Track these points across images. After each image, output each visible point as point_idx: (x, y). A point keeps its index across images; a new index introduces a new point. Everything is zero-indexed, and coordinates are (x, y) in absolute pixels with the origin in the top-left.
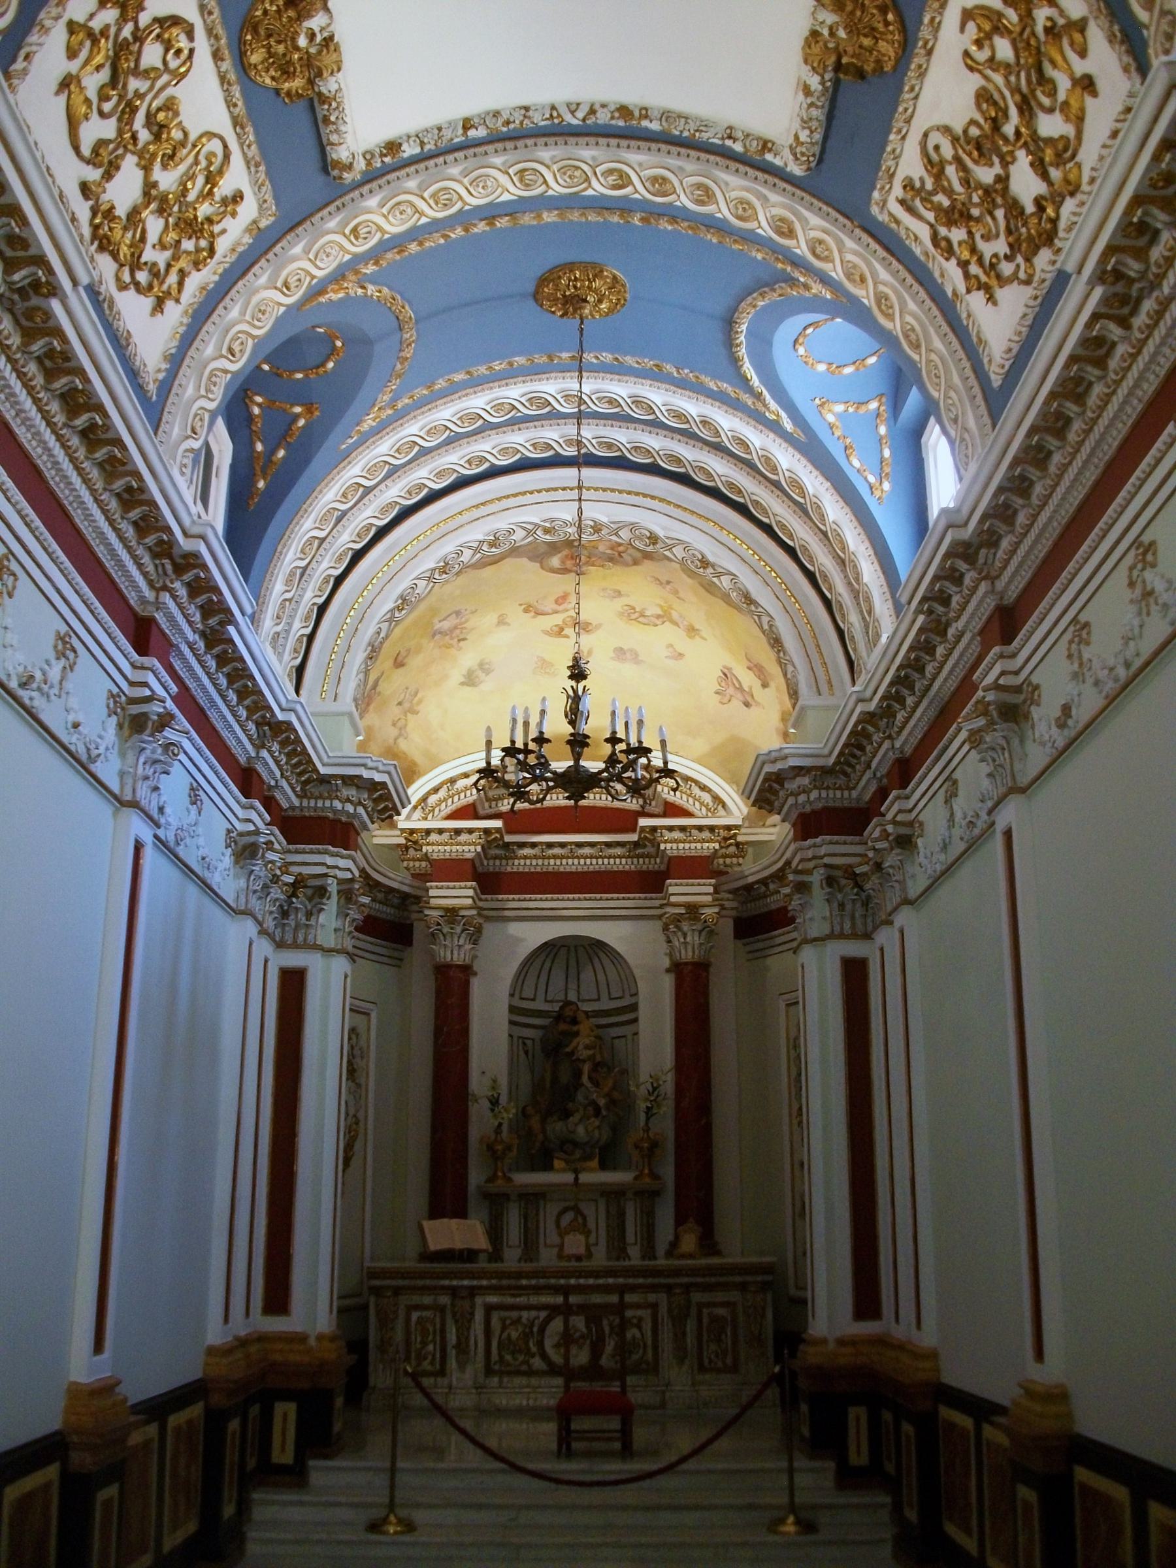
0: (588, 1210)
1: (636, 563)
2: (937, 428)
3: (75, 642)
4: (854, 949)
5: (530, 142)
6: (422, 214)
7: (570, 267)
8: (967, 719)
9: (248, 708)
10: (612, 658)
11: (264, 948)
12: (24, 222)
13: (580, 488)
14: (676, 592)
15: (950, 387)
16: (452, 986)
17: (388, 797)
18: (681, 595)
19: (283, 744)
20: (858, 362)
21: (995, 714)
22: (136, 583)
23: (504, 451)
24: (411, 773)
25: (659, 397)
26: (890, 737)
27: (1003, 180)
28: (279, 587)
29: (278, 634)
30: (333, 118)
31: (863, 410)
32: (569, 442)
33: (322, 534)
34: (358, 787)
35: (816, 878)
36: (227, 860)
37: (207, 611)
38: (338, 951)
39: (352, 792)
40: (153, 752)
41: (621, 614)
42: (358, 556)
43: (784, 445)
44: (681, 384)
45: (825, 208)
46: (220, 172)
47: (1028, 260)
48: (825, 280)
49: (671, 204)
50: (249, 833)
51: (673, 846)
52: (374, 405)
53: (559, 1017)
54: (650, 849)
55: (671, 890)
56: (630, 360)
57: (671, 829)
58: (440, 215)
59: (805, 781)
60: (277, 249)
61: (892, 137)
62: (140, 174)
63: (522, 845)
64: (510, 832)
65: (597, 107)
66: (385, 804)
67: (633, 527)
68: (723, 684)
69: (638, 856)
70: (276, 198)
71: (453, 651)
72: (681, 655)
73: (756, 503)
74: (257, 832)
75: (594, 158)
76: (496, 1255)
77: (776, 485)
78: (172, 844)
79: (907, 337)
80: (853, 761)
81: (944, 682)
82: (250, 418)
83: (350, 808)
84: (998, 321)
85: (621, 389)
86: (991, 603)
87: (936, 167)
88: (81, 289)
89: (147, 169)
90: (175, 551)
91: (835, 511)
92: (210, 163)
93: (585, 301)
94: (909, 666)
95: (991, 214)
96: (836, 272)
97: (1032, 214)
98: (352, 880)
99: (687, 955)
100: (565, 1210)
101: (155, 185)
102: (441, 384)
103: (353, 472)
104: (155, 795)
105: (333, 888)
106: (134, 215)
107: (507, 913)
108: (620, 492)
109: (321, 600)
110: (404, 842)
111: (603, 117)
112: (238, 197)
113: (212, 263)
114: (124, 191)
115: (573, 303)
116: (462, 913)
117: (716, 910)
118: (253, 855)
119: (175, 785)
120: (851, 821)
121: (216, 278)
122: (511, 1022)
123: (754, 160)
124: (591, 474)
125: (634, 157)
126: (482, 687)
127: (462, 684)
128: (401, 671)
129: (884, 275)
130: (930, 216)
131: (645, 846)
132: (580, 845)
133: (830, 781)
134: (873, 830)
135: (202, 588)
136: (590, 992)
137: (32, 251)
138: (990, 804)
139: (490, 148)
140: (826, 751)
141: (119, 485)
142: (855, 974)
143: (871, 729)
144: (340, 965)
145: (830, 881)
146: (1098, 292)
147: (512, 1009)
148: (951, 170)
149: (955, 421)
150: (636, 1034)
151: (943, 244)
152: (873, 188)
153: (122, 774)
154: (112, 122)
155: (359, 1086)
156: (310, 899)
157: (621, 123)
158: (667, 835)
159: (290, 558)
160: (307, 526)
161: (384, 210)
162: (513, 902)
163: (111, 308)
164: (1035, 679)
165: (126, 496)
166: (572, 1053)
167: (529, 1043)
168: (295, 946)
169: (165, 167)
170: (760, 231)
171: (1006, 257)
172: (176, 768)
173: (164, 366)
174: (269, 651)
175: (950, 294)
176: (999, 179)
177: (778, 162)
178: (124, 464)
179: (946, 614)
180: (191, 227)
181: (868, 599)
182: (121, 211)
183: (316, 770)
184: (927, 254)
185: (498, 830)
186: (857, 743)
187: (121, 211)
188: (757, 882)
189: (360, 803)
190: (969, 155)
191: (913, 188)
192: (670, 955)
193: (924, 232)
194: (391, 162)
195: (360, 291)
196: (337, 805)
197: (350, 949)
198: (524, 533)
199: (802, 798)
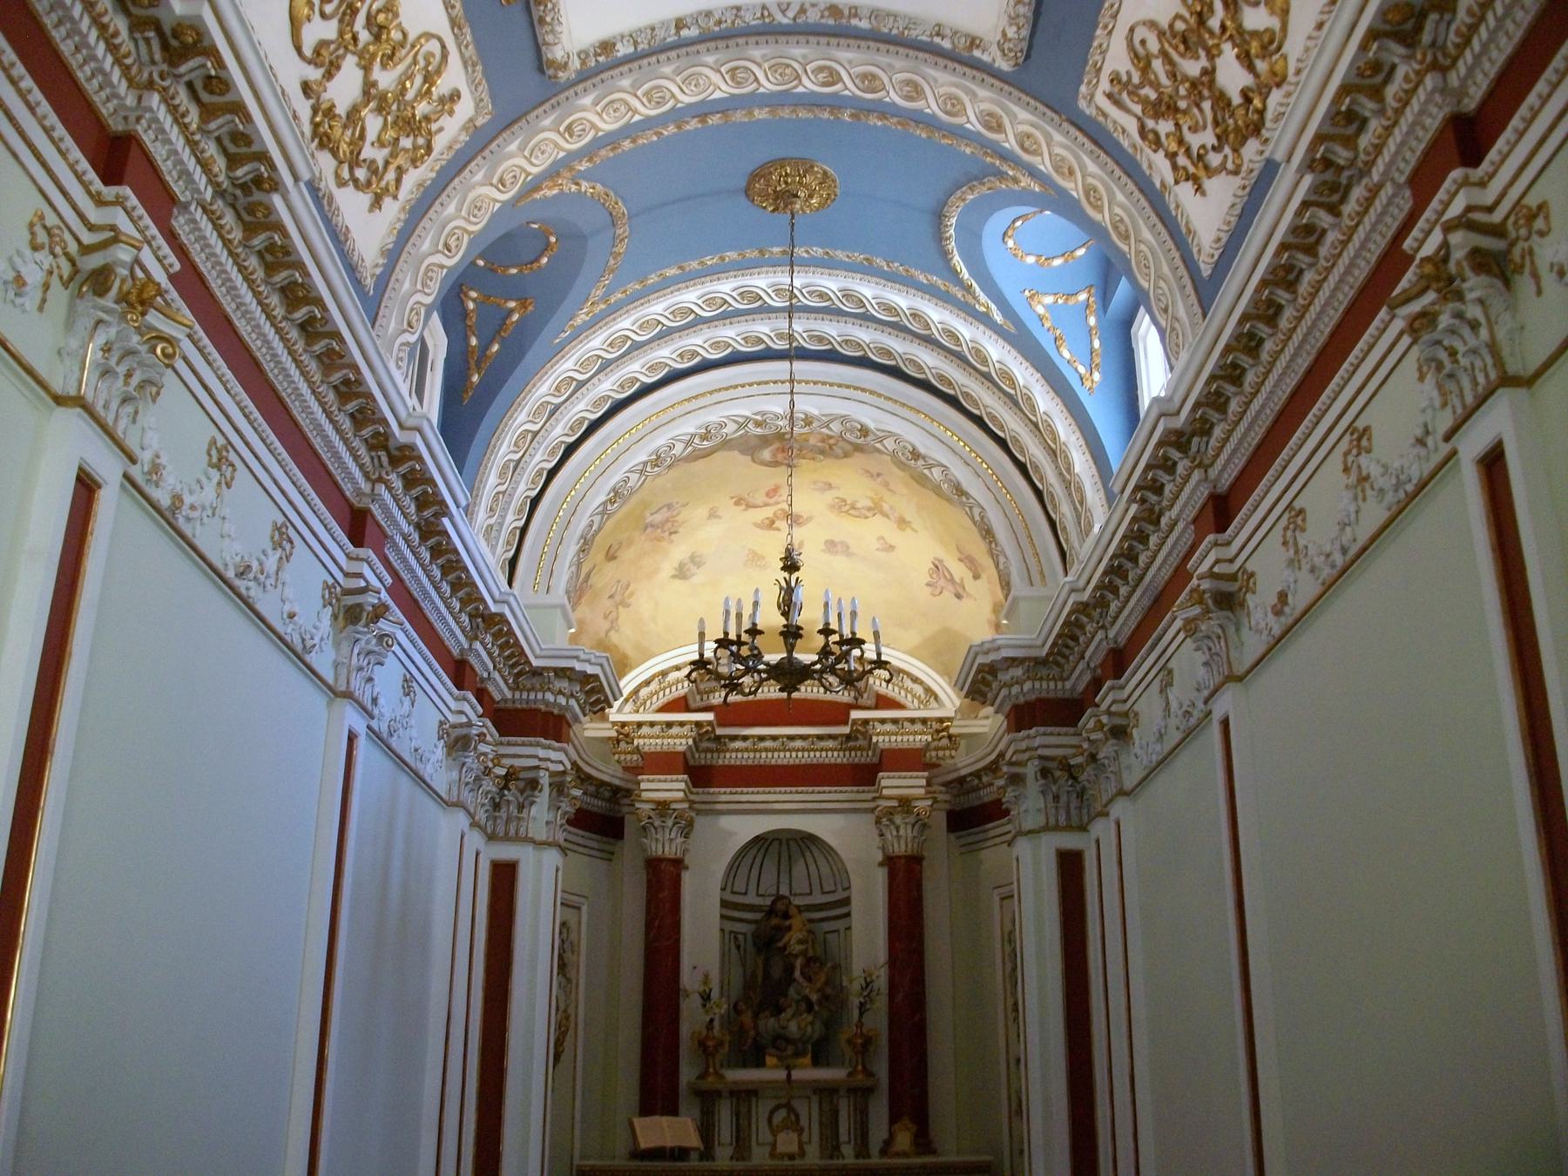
0: (801, 1107)
1: (846, 455)
2: (1147, 317)
3: (291, 532)
4: (1070, 841)
5: (741, 41)
6: (636, 112)
7: (781, 162)
8: (1181, 608)
9: (461, 600)
11: (475, 840)
12: (248, 118)
13: (792, 381)
14: (886, 485)
15: (1159, 277)
16: (663, 881)
17: (601, 689)
18: (892, 486)
19: (496, 636)
20: (1067, 254)
21: (1210, 602)
22: (352, 474)
23: (716, 345)
24: (623, 666)
25: (868, 290)
26: (1103, 627)
27: (1209, 73)
28: (492, 479)
29: (491, 526)
30: (548, 19)
31: (1072, 302)
32: (780, 336)
33: (535, 428)
34: (570, 680)
35: (1031, 770)
36: (440, 752)
37: (422, 503)
38: (550, 844)
39: (563, 684)
40: (368, 642)
41: (832, 507)
42: (570, 449)
43: (994, 337)
44: (891, 278)
45: (1032, 102)
46: (438, 72)
47: (1235, 150)
48: (1033, 173)
49: (880, 100)
50: (461, 725)
51: (884, 739)
52: (587, 300)
53: (771, 911)
54: (861, 742)
55: (884, 783)
56: (840, 255)
57: (883, 721)
58: (653, 113)
59: (1018, 672)
60: (493, 146)
61: (1099, 32)
62: (360, 74)
63: (734, 738)
64: (722, 724)
65: (807, 6)
66: (596, 695)
67: (844, 419)
69: (850, 750)
70: (493, 97)
71: (664, 544)
72: (892, 548)
73: (967, 395)
74: (469, 724)
75: (804, 57)
76: (707, 1154)
77: (987, 377)
78: (385, 735)
79: (1116, 228)
80: (1067, 652)
81: (1158, 571)
82: (465, 314)
83: (562, 701)
84: (1206, 211)
85: (832, 284)
86: (1204, 492)
87: (1142, 62)
88: (302, 185)
89: (367, 69)
90: (391, 444)
91: (1045, 402)
92: (428, 63)
93: (796, 196)
94: (1122, 555)
95: (1198, 106)
96: (1044, 165)
97: (1240, 106)
98: (564, 773)
99: (900, 849)
100: (777, 1108)
101: (374, 84)
102: (653, 279)
103: (567, 366)
104: (369, 686)
105: (545, 780)
106: (354, 114)
107: (718, 807)
108: (831, 385)
109: (534, 493)
110: (614, 734)
111: (813, 16)
112: (455, 96)
113: (429, 161)
114: (344, 89)
115: (783, 199)
116: (674, 806)
117: (929, 802)
118: (466, 747)
119: (388, 677)
120: (1066, 712)
121: (433, 175)
122: (722, 917)
123: (961, 56)
124: (802, 368)
125: (845, 55)
126: (695, 580)
127: (674, 577)
128: (613, 564)
129: (1092, 167)
130: (1138, 109)
131: (857, 739)
132: (791, 738)
133: (1044, 672)
134: (1088, 721)
135: (416, 480)
136: (802, 885)
137: (255, 148)
138: (1206, 693)
139: (702, 47)
140: (1039, 642)
141: (336, 377)
142: (1070, 866)
143: (1085, 619)
144: (552, 858)
145: (1045, 773)
146: (1308, 180)
147: (725, 904)
148: (1157, 65)
149: (1166, 310)
150: (849, 928)
151: (1151, 136)
152: (1081, 82)
153: (336, 665)
154: (334, 24)
155: (569, 980)
156: (522, 792)
157: (831, 22)
158: (879, 728)
159: (504, 451)
160: (521, 419)
161: (598, 109)
162: (724, 795)
163: (330, 204)
164: (1250, 567)
165: (343, 389)
166: (785, 948)
167: (741, 937)
168: (507, 838)
169: (384, 66)
170: (968, 126)
171: (1213, 148)
172: (390, 660)
173: (381, 261)
174: (483, 544)
175: (1158, 185)
176: (1205, 72)
177: (986, 58)
178: (342, 357)
179: (1159, 503)
180: (409, 125)
181: (1080, 490)
182: (341, 110)
183: (528, 662)
184: (1134, 146)
185: (710, 723)
186: (1071, 633)
187: (341, 110)
188: (971, 774)
189: (572, 695)
190: (1176, 48)
191: (1119, 82)
192: (883, 848)
193: (1131, 125)
194: (605, 61)
195: (574, 188)
196: (550, 697)
197: (562, 842)
198: (735, 426)
199: (1015, 689)
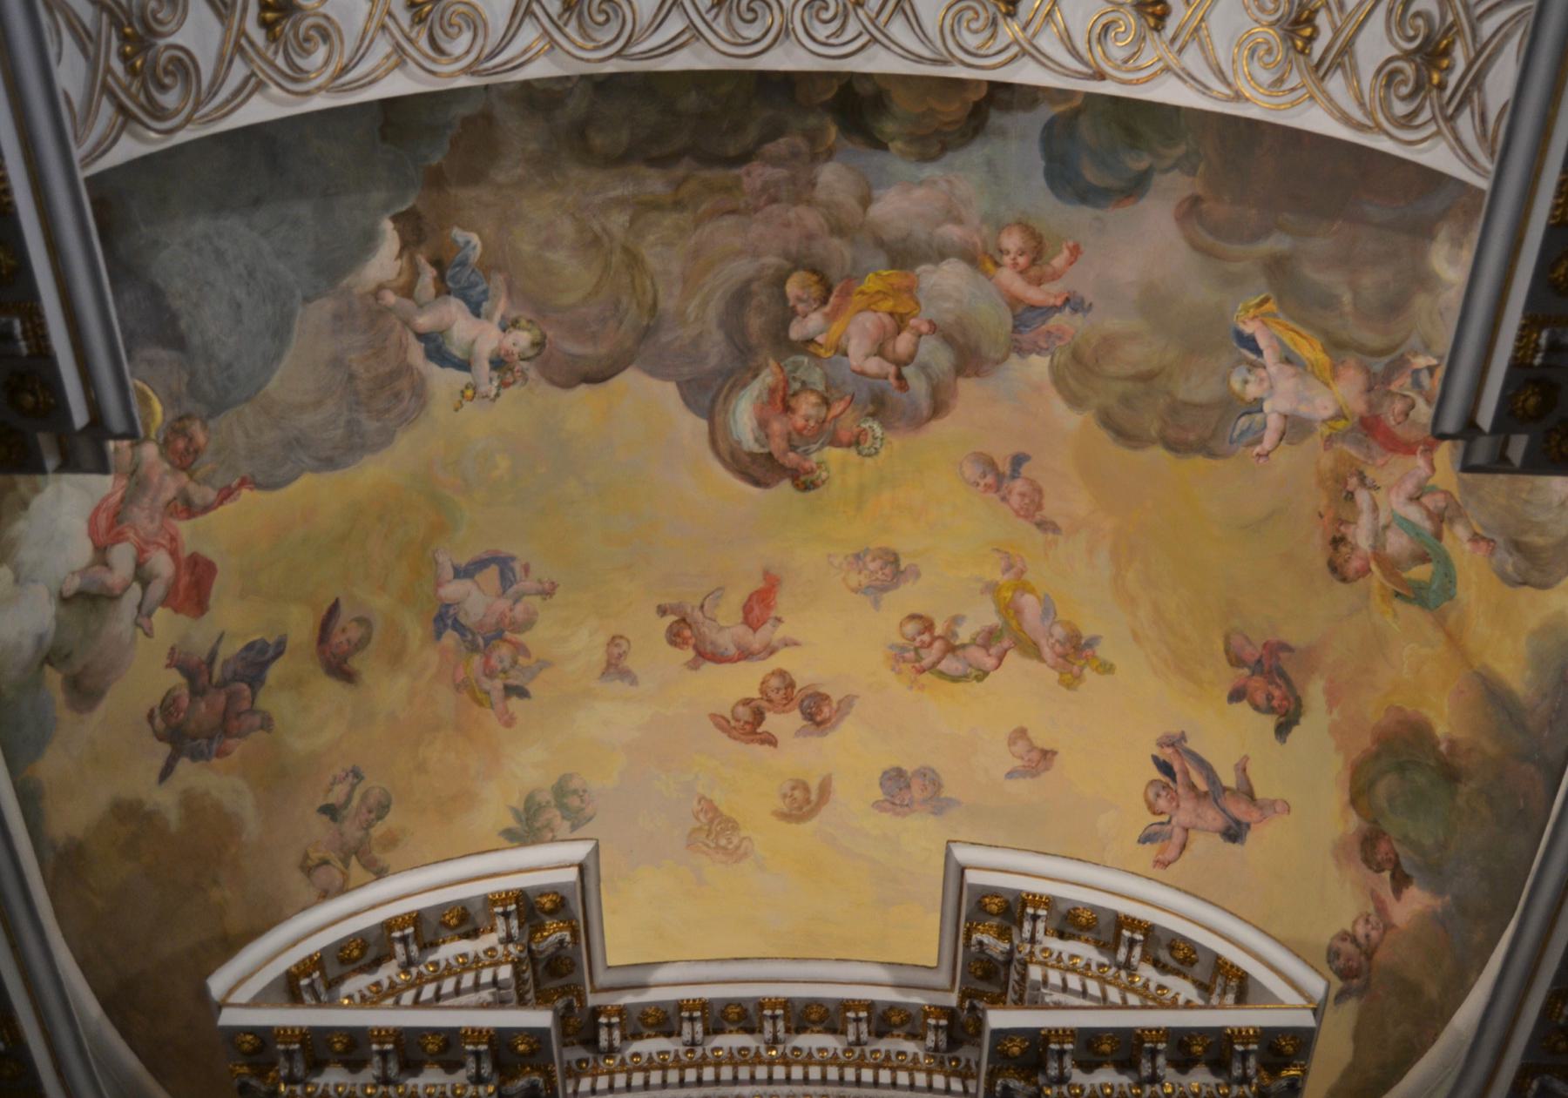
10: (877, 805)
14: (1033, 510)
68: (1162, 803)
72: (1047, 755)
